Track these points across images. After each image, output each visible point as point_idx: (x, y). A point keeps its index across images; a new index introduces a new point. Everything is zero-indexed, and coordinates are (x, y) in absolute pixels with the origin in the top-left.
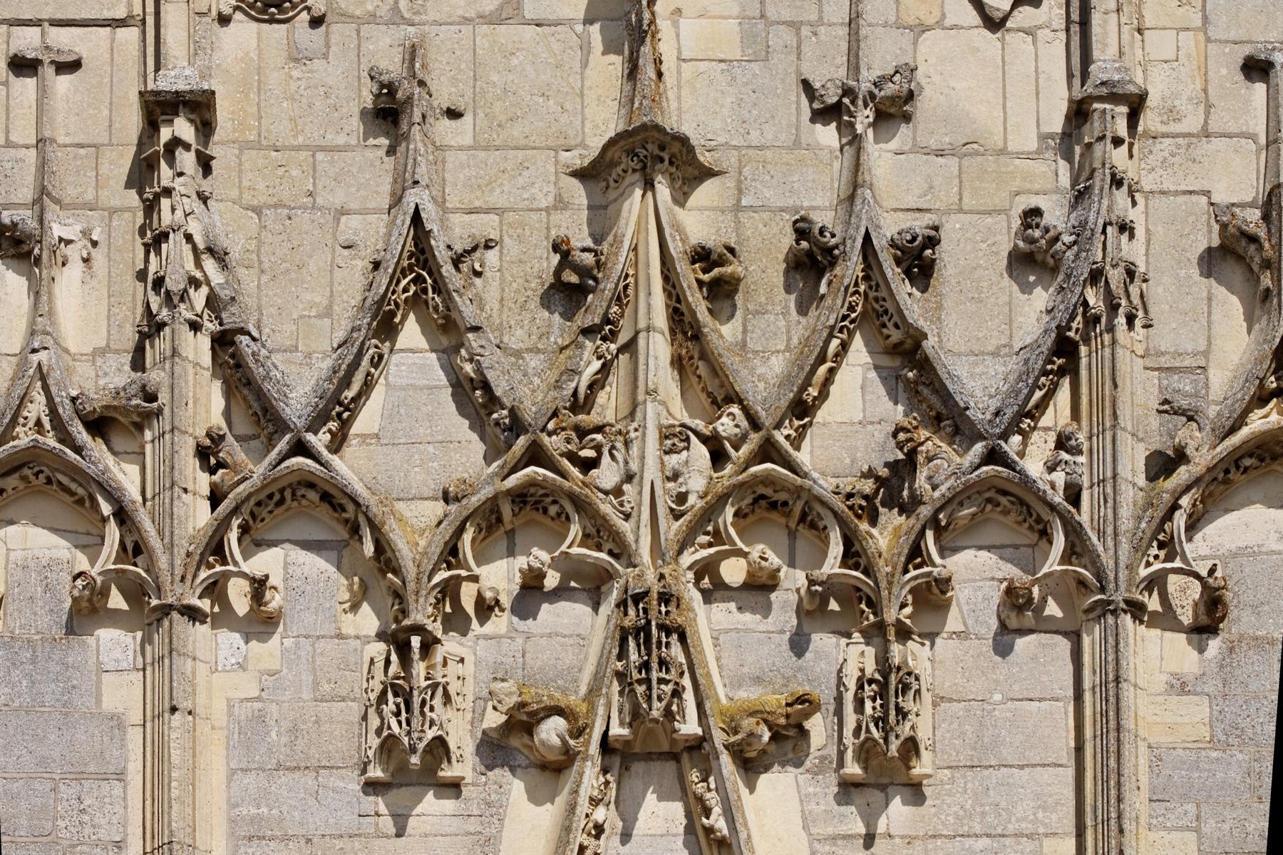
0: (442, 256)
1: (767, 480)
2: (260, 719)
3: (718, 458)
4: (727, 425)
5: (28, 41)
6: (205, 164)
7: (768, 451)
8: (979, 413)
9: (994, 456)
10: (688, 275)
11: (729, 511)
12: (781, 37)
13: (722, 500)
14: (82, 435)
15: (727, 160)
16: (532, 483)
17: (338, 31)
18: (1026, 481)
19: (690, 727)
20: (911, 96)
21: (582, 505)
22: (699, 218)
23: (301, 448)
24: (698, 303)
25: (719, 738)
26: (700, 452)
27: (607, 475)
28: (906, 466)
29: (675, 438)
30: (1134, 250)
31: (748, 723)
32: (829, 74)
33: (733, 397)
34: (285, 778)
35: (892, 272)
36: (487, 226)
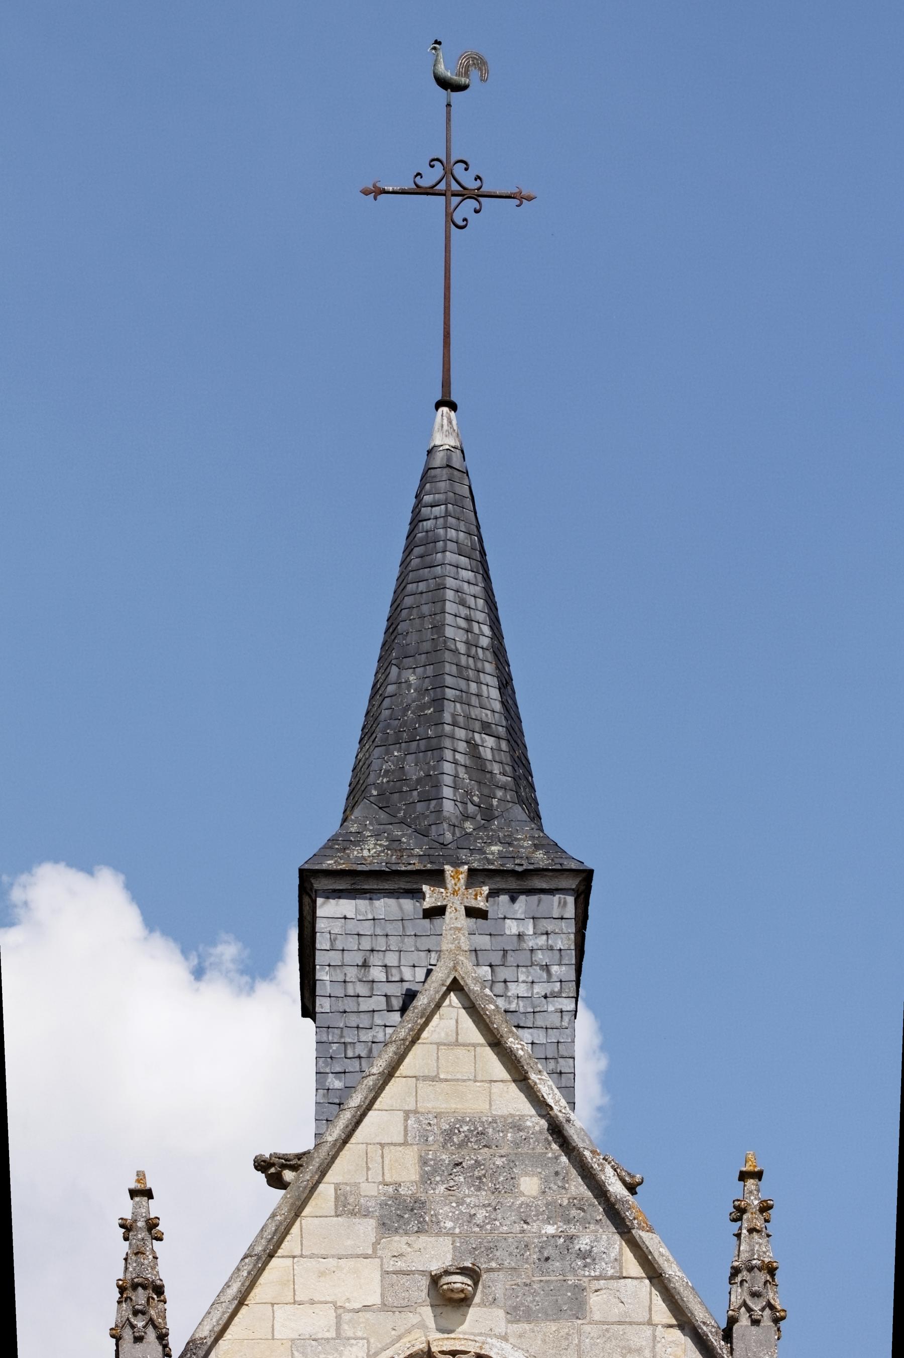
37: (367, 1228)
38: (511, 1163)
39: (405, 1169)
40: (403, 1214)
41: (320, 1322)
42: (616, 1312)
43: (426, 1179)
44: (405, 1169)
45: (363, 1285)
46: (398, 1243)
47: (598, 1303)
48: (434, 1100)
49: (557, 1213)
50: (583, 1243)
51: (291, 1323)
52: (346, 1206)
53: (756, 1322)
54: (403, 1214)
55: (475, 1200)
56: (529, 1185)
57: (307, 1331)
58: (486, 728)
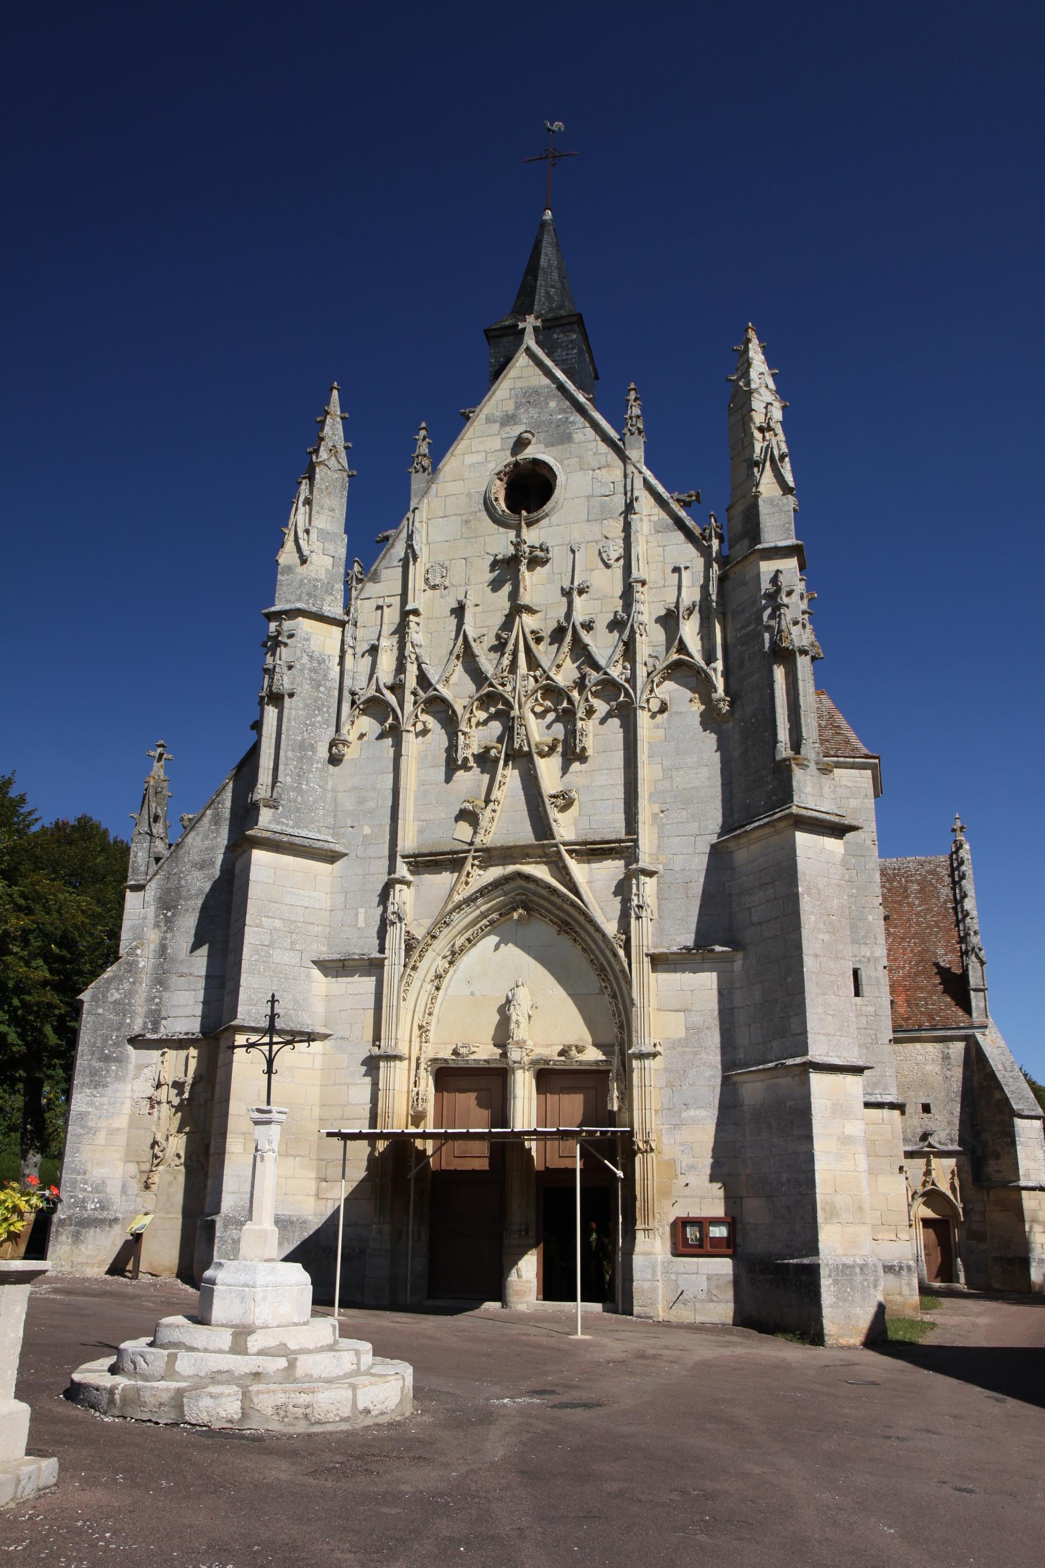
0: (471, 639)
1: (548, 685)
2: (426, 755)
3: (536, 681)
4: (538, 673)
5: (380, 602)
6: (418, 624)
7: (549, 678)
8: (602, 662)
9: (606, 673)
10: (529, 637)
11: (540, 692)
12: (557, 577)
13: (536, 691)
14: (385, 691)
15: (543, 608)
16: (489, 692)
17: (452, 590)
18: (614, 679)
19: (526, 749)
20: (588, 587)
21: (502, 696)
22: (529, 622)
23: (435, 689)
24: (532, 644)
25: (534, 750)
26: (532, 679)
27: (509, 688)
28: (583, 677)
29: (525, 678)
30: (641, 618)
31: (541, 747)
32: (567, 585)
33: (540, 666)
34: (431, 769)
35: (579, 628)
36: (484, 631)
37: (496, 427)
38: (546, 398)
39: (510, 407)
40: (508, 420)
41: (480, 458)
42: (583, 438)
43: (517, 408)
44: (510, 407)
45: (496, 443)
46: (507, 429)
47: (578, 437)
48: (520, 384)
49: (564, 411)
50: (571, 419)
51: (470, 459)
52: (489, 420)
53: (632, 434)
54: (508, 420)
55: (533, 412)
56: (553, 404)
57: (475, 461)
58: (552, 286)
